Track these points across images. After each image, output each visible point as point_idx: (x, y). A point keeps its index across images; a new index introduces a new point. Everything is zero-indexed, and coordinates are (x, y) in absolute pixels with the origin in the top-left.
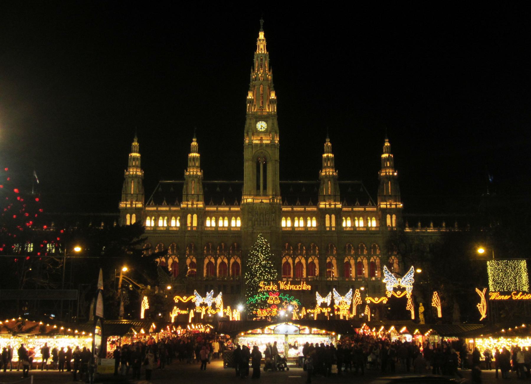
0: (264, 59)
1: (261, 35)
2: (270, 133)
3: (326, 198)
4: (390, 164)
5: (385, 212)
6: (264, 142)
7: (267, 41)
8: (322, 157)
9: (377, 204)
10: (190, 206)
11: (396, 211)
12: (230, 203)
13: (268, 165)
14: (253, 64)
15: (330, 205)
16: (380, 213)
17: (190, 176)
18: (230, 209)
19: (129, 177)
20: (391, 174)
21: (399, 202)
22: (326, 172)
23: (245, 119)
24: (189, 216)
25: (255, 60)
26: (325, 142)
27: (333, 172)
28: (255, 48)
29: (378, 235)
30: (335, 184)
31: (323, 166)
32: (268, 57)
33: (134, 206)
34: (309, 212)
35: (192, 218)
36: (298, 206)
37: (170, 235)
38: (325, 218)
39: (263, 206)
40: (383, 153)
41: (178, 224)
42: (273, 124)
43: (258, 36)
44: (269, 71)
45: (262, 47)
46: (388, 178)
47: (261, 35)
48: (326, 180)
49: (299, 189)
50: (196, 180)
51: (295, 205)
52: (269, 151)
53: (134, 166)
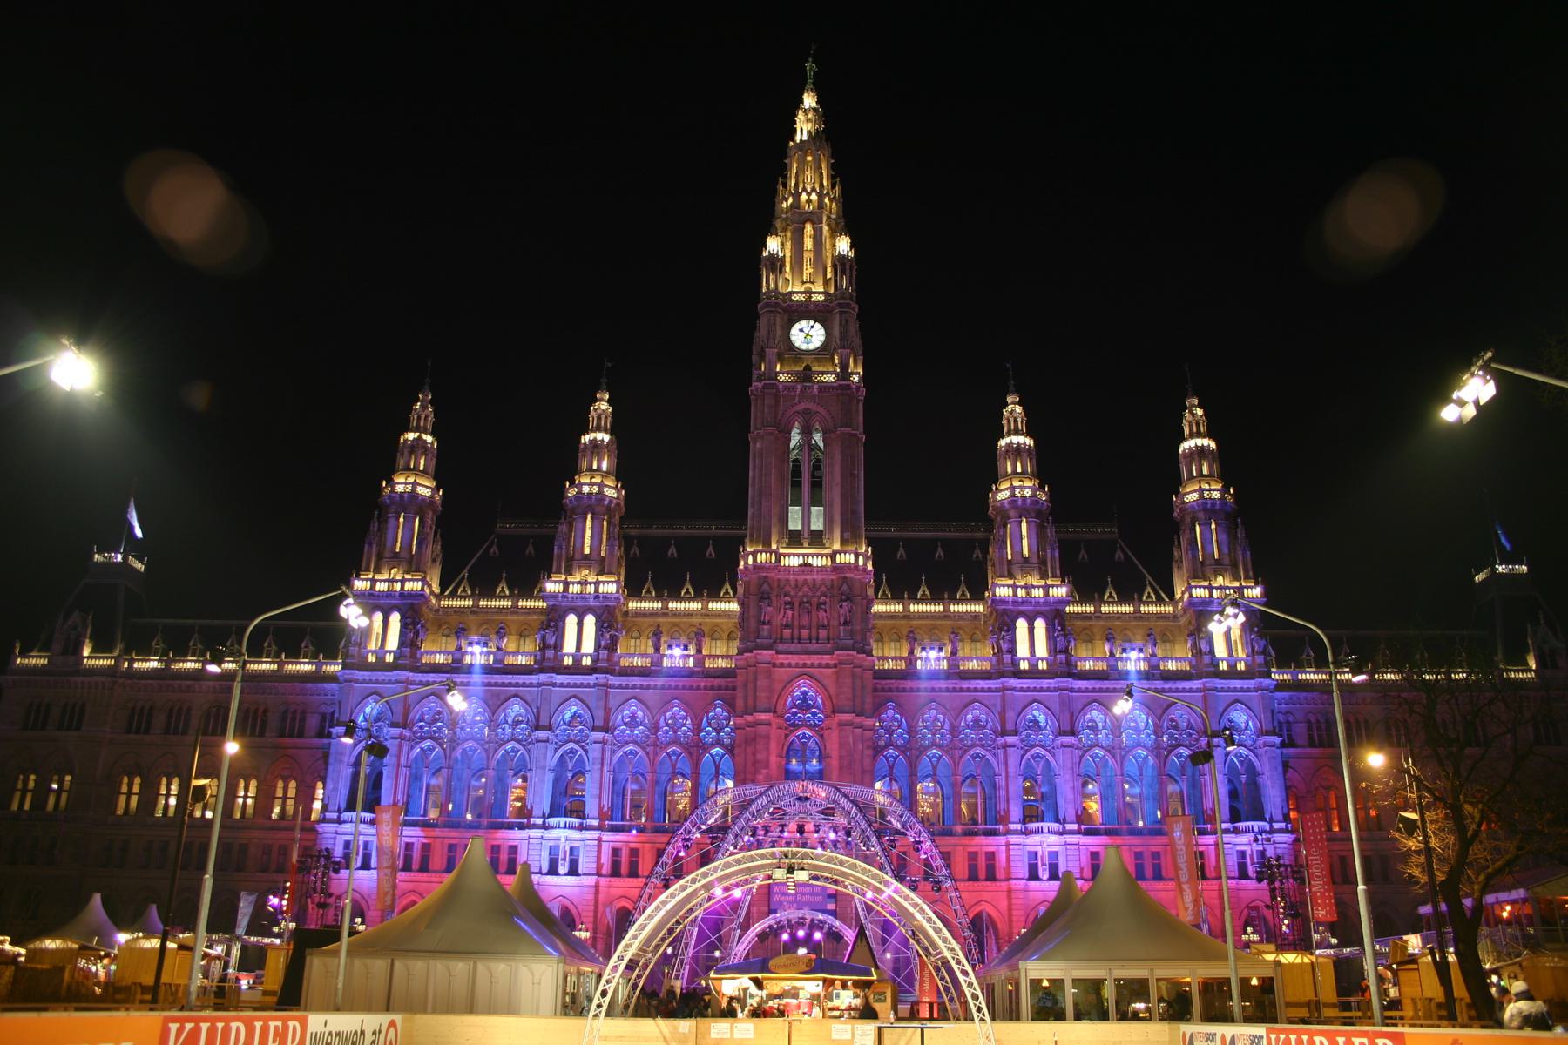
3: (1016, 569)
4: (1210, 468)
9: (1171, 595)
12: (709, 588)
14: (783, 172)
15: (1027, 587)
18: (705, 608)
19: (393, 503)
27: (1034, 489)
34: (961, 616)
36: (923, 601)
40: (1183, 439)
42: (845, 325)
44: (833, 187)
46: (1207, 509)
47: (809, 100)
48: (1012, 513)
49: (930, 542)
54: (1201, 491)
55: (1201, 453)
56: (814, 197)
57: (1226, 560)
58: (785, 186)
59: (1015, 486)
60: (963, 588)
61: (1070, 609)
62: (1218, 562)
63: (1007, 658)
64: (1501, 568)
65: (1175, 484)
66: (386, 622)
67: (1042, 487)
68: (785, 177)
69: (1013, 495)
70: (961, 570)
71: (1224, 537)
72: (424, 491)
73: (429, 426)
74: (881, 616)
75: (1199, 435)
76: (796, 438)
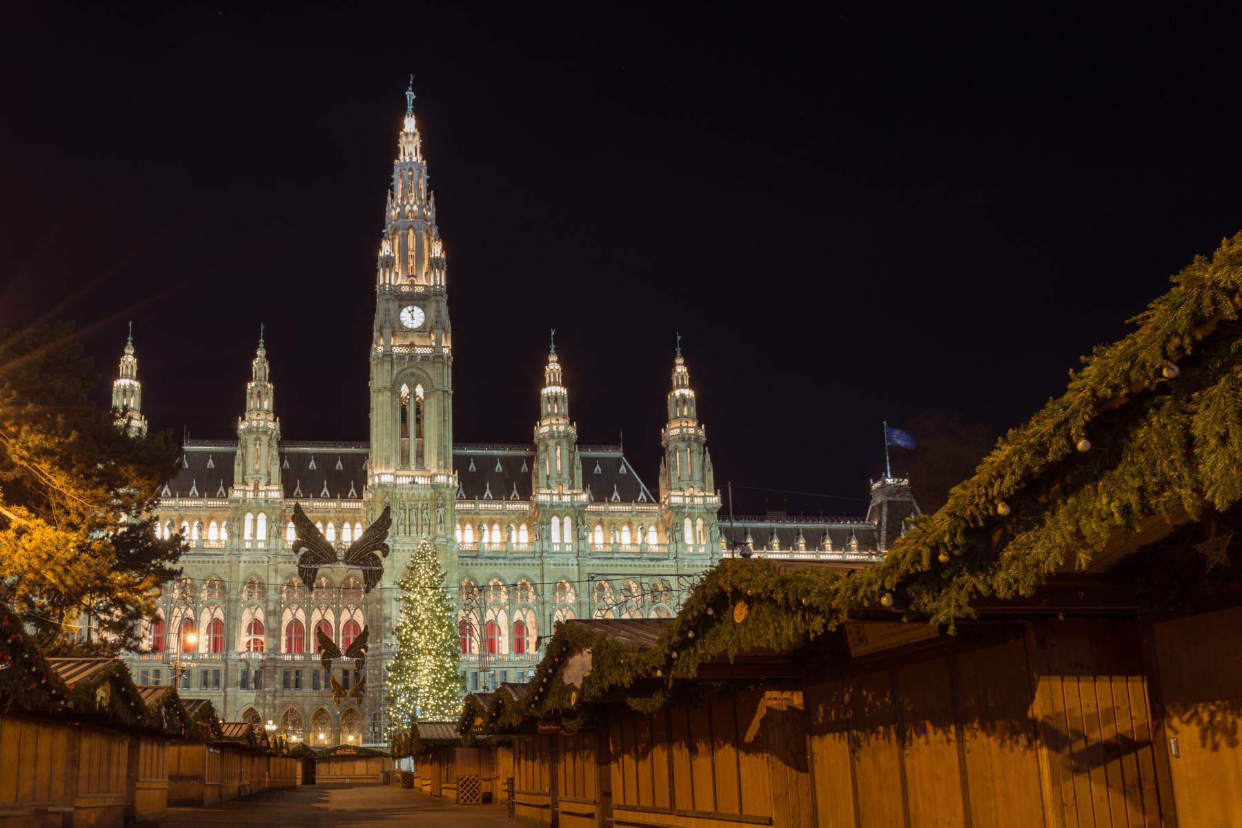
0: (416, 173)
1: (410, 124)
2: (430, 332)
3: (553, 485)
5: (678, 510)
6: (419, 351)
7: (421, 137)
8: (539, 395)
10: (250, 495)
14: (392, 190)
15: (560, 495)
17: (250, 431)
20: (692, 431)
24: (249, 517)
26: (547, 363)
28: (395, 152)
29: (665, 562)
31: (544, 412)
32: (424, 171)
35: (255, 521)
37: (206, 559)
38: (549, 523)
39: (416, 492)
41: (224, 535)
42: (438, 311)
43: (403, 126)
44: (428, 198)
46: (684, 438)
47: (410, 124)
48: (551, 443)
50: (265, 439)
51: (481, 498)
54: (681, 427)
56: (415, 208)
57: (697, 476)
59: (554, 424)
60: (515, 492)
61: (590, 508)
63: (546, 544)
64: (890, 481)
65: (664, 420)
67: (571, 424)
69: (551, 429)
70: (518, 482)
76: (405, 390)
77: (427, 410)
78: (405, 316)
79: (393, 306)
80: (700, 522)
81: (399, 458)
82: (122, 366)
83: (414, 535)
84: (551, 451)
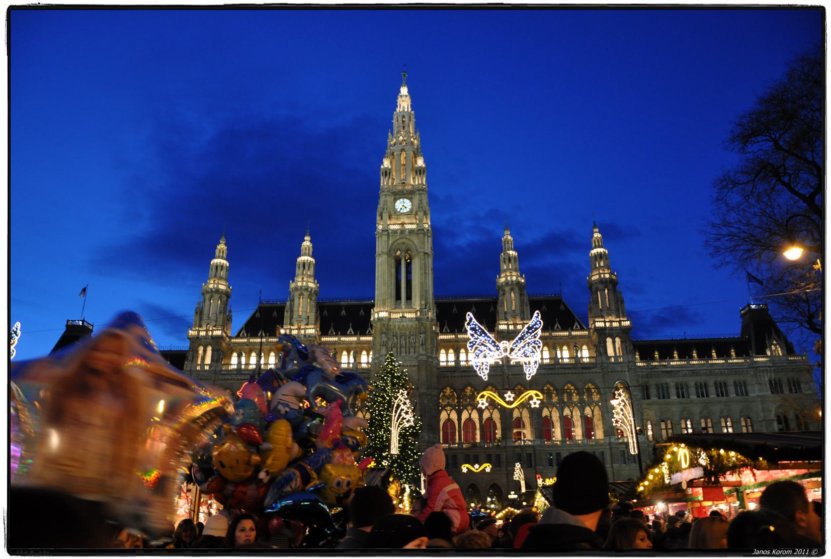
1: (404, 91)
3: (508, 317)
5: (603, 333)
6: (408, 227)
9: (587, 325)
11: (623, 332)
13: (413, 261)
15: (515, 325)
16: (595, 337)
17: (296, 289)
18: (358, 339)
20: (607, 276)
21: (623, 316)
22: (506, 276)
23: (377, 197)
25: (394, 121)
27: (517, 276)
28: (395, 106)
30: (521, 295)
32: (412, 117)
33: (210, 333)
39: (405, 324)
42: (421, 201)
44: (416, 133)
45: (404, 103)
46: (602, 281)
47: (404, 91)
48: (507, 289)
50: (306, 294)
52: (415, 239)
53: (215, 276)
54: (600, 274)
55: (600, 256)
57: (613, 307)
58: (392, 133)
62: (609, 309)
66: (205, 351)
67: (521, 276)
68: (392, 129)
71: (612, 297)
72: (222, 287)
73: (225, 256)
74: (442, 340)
75: (599, 247)
77: (413, 266)
78: (399, 205)
79: (390, 199)
80: (618, 340)
81: (393, 300)
82: (217, 251)
83: (403, 354)
84: (507, 294)
